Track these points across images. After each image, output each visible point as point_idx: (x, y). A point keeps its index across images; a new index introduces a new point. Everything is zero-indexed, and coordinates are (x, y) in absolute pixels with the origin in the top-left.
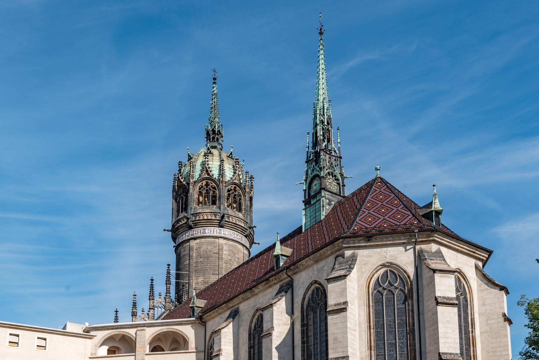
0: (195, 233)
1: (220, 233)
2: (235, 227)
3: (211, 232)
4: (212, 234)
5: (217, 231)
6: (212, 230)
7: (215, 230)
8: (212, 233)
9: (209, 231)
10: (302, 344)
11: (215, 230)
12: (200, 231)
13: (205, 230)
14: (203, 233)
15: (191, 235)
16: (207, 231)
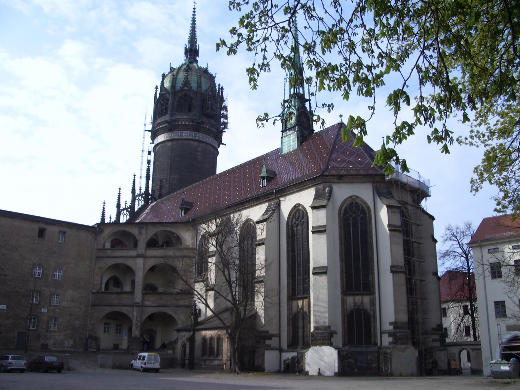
0: (174, 136)
1: (195, 136)
2: (207, 132)
3: (187, 135)
4: (188, 137)
5: (192, 134)
6: (189, 133)
7: (191, 134)
8: (188, 136)
9: (186, 134)
10: (287, 252)
11: (191, 134)
12: (178, 134)
13: (182, 133)
14: (180, 136)
15: (170, 137)
16: (184, 134)
